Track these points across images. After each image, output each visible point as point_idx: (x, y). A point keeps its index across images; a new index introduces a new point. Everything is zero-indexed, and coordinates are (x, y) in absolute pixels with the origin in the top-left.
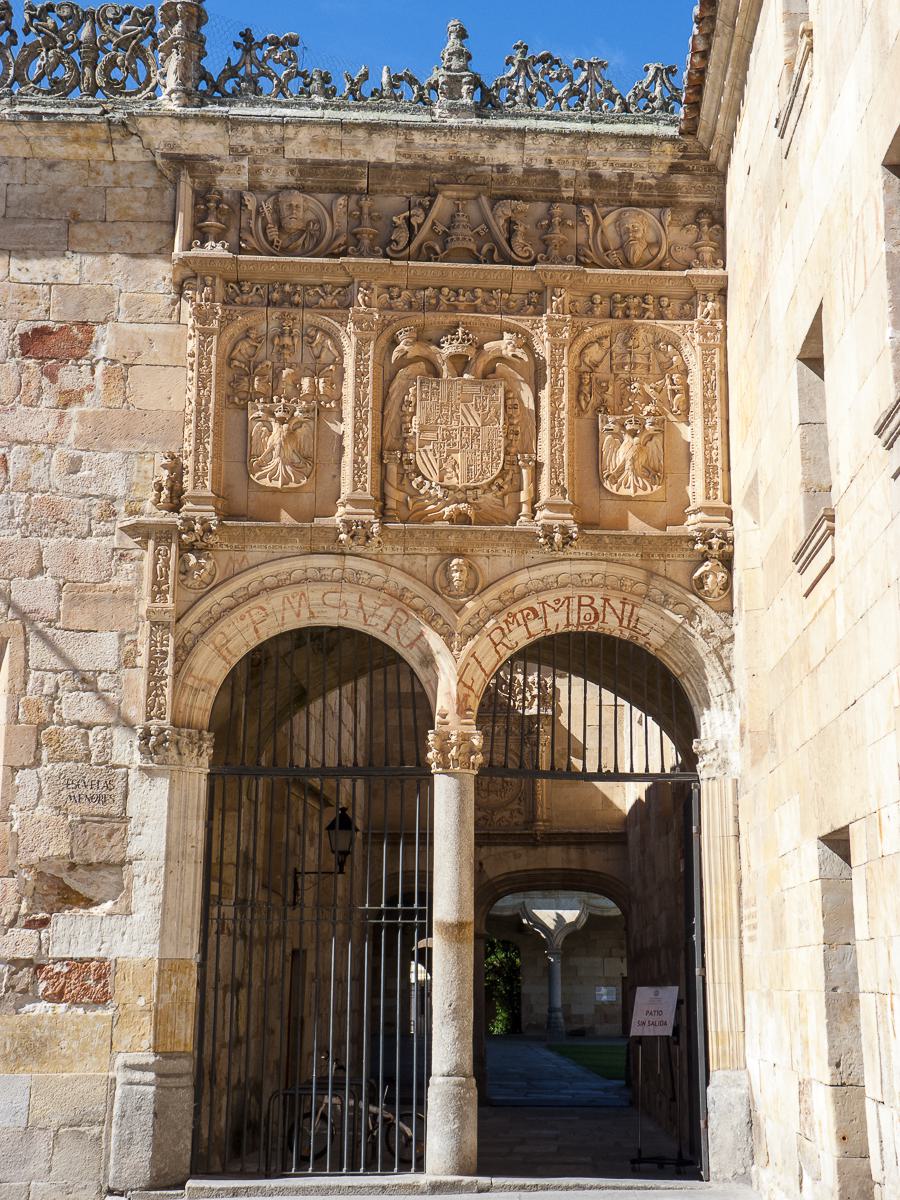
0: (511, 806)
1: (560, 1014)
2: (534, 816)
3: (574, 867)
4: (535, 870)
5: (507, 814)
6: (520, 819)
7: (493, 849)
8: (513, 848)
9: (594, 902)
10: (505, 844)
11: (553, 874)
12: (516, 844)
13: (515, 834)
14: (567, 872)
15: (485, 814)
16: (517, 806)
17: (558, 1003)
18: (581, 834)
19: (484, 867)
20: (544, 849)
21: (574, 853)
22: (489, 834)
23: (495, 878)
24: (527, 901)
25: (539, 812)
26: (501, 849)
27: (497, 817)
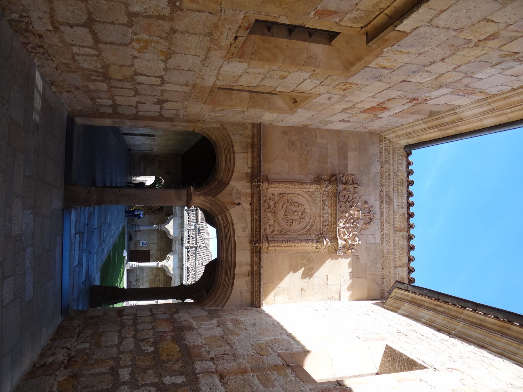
1: (137, 229)
2: (271, 241)
5: (271, 222)
6: (268, 231)
7: (249, 213)
8: (249, 226)
9: (177, 242)
10: (252, 220)
12: (252, 229)
13: (260, 228)
14: (233, 263)
15: (272, 207)
16: (277, 229)
17: (141, 228)
18: (260, 274)
19: (237, 206)
20: (249, 248)
21: (246, 269)
22: (260, 210)
23: (230, 214)
24: (178, 217)
25: (274, 245)
26: (249, 219)
27: (269, 215)
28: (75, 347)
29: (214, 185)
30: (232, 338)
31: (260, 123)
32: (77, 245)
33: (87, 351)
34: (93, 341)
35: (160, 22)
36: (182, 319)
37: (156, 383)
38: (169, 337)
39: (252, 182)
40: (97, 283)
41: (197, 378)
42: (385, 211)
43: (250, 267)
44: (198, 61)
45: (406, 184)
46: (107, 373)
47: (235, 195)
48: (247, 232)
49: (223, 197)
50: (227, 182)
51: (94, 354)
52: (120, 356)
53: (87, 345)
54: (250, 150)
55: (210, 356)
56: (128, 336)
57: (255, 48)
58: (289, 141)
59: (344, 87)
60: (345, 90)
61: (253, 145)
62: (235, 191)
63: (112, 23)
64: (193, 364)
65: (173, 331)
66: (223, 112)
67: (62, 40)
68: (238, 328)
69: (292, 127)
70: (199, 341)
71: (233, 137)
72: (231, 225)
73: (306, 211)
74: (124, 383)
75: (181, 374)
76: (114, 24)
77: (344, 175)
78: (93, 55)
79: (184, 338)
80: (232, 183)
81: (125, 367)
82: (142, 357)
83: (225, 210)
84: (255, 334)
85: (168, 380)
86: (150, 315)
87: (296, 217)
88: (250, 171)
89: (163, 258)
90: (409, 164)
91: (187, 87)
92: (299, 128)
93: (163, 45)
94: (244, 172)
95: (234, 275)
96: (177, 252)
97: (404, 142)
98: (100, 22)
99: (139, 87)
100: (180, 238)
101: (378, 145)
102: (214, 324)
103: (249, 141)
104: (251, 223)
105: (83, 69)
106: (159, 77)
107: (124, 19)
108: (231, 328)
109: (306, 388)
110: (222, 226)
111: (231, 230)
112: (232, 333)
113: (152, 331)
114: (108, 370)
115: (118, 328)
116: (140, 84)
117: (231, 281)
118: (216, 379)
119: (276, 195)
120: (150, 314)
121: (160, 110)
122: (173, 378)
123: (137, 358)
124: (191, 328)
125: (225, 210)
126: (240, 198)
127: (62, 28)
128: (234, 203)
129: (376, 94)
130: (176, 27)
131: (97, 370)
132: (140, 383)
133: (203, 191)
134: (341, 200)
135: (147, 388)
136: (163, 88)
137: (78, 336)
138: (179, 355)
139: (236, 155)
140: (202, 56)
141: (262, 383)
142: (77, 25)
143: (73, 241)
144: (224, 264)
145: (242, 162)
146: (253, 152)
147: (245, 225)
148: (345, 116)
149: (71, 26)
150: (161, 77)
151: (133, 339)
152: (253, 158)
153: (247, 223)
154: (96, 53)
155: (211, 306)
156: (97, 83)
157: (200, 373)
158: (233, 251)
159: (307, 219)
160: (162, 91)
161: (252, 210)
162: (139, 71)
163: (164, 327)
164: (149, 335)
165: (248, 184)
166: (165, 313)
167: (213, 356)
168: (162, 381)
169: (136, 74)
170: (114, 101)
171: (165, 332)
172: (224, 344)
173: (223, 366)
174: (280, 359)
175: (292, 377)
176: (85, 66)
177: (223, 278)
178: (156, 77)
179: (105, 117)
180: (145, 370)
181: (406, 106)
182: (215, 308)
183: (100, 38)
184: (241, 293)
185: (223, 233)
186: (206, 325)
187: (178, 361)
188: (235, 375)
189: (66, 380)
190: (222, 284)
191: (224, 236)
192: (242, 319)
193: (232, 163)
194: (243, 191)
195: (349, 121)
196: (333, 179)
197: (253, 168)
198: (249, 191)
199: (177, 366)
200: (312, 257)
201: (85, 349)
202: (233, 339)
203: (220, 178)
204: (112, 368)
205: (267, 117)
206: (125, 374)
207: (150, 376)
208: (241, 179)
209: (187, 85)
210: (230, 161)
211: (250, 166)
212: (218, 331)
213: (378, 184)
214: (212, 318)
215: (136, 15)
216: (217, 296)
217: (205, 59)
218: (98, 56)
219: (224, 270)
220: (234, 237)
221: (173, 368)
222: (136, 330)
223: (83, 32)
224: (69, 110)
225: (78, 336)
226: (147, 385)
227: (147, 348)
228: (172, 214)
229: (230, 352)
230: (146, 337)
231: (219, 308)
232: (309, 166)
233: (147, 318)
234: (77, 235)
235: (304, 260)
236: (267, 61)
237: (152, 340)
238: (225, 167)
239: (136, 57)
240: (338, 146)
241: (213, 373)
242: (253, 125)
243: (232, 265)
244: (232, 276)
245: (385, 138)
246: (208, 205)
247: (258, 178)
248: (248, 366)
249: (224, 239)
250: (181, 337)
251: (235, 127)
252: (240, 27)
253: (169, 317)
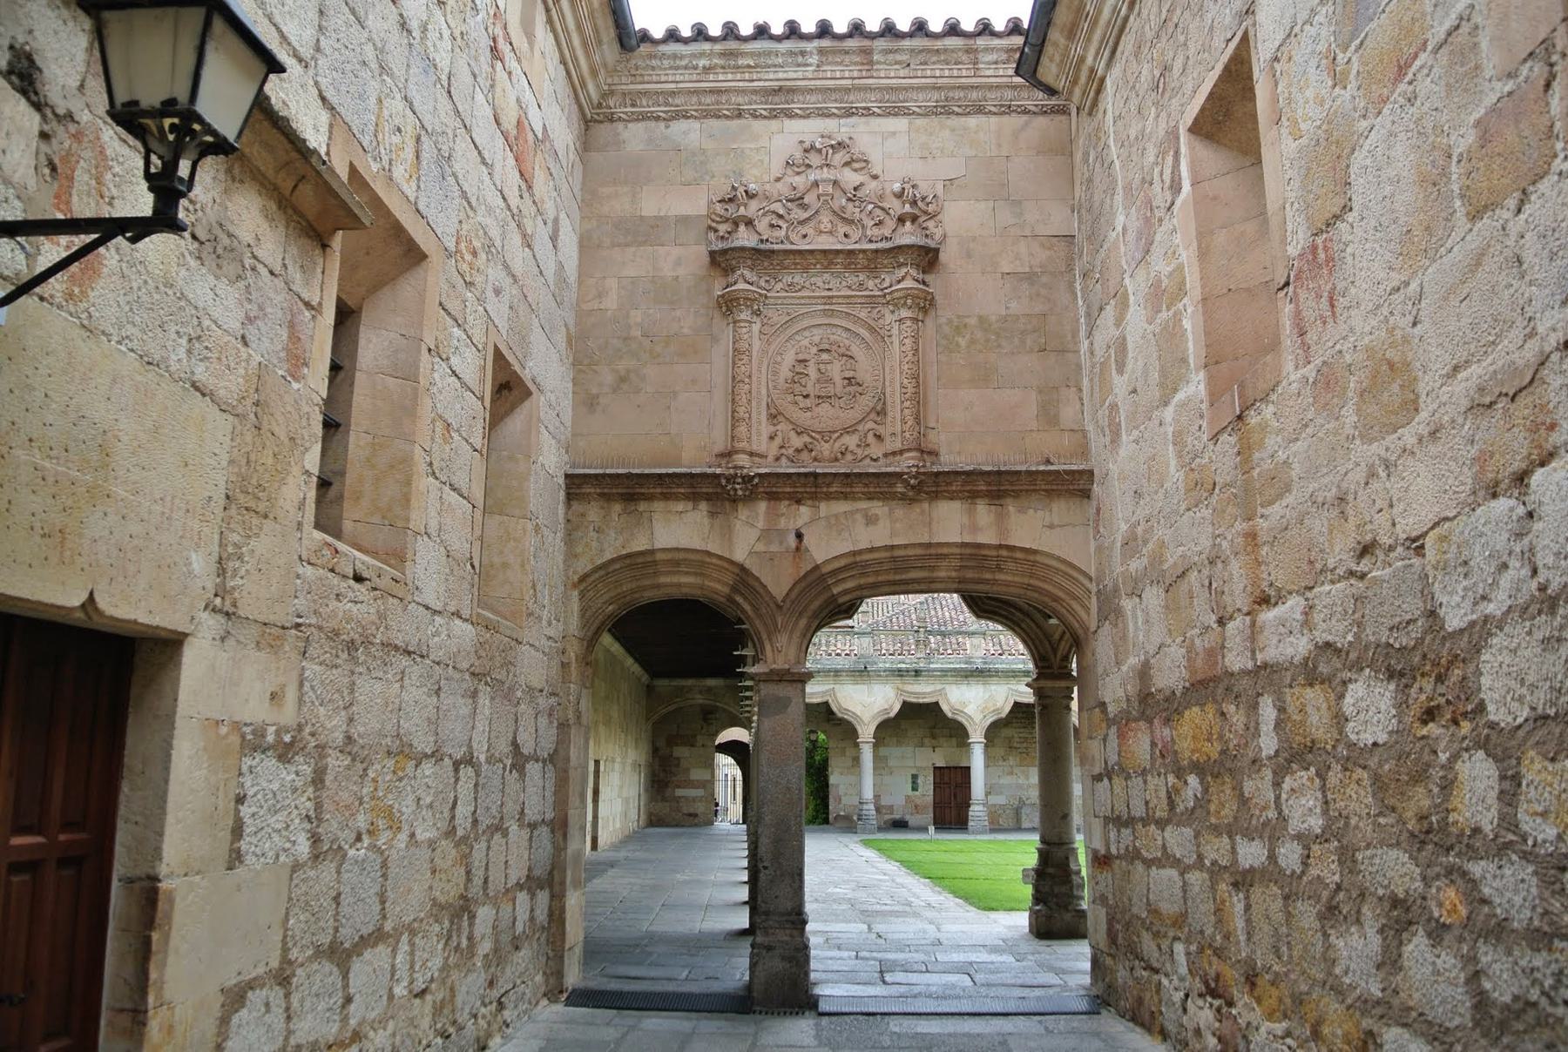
0: (860, 428)
3: (982, 539)
4: (906, 546)
7: (823, 506)
8: (863, 505)
9: (909, 688)
10: (845, 497)
11: (945, 556)
12: (870, 497)
14: (968, 551)
15: (808, 439)
16: (870, 425)
18: (999, 473)
20: (926, 505)
21: (984, 512)
22: (815, 475)
26: (841, 507)
28: (1182, 979)
29: (747, 607)
30: (1171, 561)
31: (567, 476)
32: (913, 978)
33: (1193, 948)
34: (1171, 934)
35: (329, 779)
36: (1121, 693)
37: (1275, 773)
38: (1166, 732)
39: (734, 501)
40: (1022, 920)
41: (1265, 666)
42: (813, 101)
43: (978, 501)
44: (415, 671)
45: (732, 45)
46: (1247, 898)
47: (774, 548)
48: (878, 511)
49: (778, 581)
50: (737, 571)
51: (1202, 932)
52: (1207, 863)
53: (1179, 948)
54: (642, 506)
55: (1215, 626)
56: (1160, 842)
57: (376, 519)
58: (614, 391)
59: (468, 257)
60: (475, 254)
61: (630, 498)
62: (760, 547)
63: (337, 899)
64: (1232, 674)
65: (1150, 721)
66: (539, 587)
67: (382, 1022)
68: (1145, 542)
69: (575, 382)
70: (1176, 652)
71: (608, 556)
72: (858, 559)
73: (816, 339)
74: (1272, 857)
75: (1254, 706)
76: (339, 894)
77: (710, 228)
78: (412, 944)
79: (1168, 693)
80: (740, 555)
81: (1234, 851)
82: (1213, 808)
83: (817, 574)
84: (1161, 495)
85: (1268, 743)
86: (1110, 779)
87: (836, 370)
88: (703, 506)
89: (955, 731)
90: (672, 35)
91: (481, 694)
92: (576, 363)
93: (381, 768)
94: (706, 521)
95: (1000, 546)
96: (939, 687)
97: (610, 51)
98: (336, 930)
99: (485, 821)
100: (898, 681)
101: (620, 126)
102: (1134, 608)
103: (617, 507)
104: (854, 499)
105: (445, 968)
106: (456, 770)
107: (327, 870)
108: (1145, 560)
109: (1292, 378)
110: (862, 581)
111: (876, 555)
112: (1157, 559)
113: (1149, 777)
114: (1241, 895)
115: (1140, 867)
116: (475, 822)
117: (1019, 555)
118: (1268, 616)
119: (772, 429)
120: (1106, 780)
121: (537, 761)
122: (1264, 728)
123: (1213, 820)
124: (1144, 673)
125: (817, 574)
126: (782, 533)
127: (353, 1022)
128: (798, 549)
129: (484, 162)
130: (339, 737)
131: (1240, 924)
132: (1272, 814)
133: (764, 636)
134: (783, 233)
135: (1284, 796)
136: (482, 758)
137: (1157, 971)
138: (1211, 709)
139: (658, 545)
140: (405, 661)
141: (1280, 496)
142: (346, 986)
143: (902, 989)
144: (970, 575)
145: (677, 529)
146: (650, 498)
147: (858, 516)
148: (542, 234)
149: (348, 1000)
150: (457, 765)
151: (1169, 828)
152: (666, 497)
153: (852, 513)
154: (405, 938)
155: (1087, 610)
156: (477, 933)
157: (1254, 658)
158: (933, 551)
159: (840, 336)
160: (490, 760)
161: (815, 497)
162: (443, 825)
163: (1141, 745)
164: (1158, 786)
165: (743, 513)
166: (1105, 740)
167: (1214, 618)
168: (1270, 758)
169: (451, 832)
170: (520, 886)
171: (1153, 744)
172: (1183, 586)
173: (1238, 598)
174: (1224, 437)
175: (1268, 410)
176: (437, 962)
177: (1009, 578)
178: (457, 780)
179: (563, 910)
180: (1244, 801)
181: (512, 64)
182: (1094, 599)
183: (371, 928)
184: (1051, 527)
185: (880, 578)
186: (1136, 629)
187: (1223, 714)
188: (1259, 564)
189: (1259, 1001)
190: (1026, 580)
191: (891, 577)
192: (1124, 527)
193: (681, 556)
194: (761, 524)
195: (556, 220)
196: (722, 261)
197: (694, 497)
198: (762, 506)
199: (1237, 717)
200: (950, 321)
201: (1188, 954)
202: (1171, 559)
203: (726, 590)
204: (1235, 885)
205: (551, 460)
206: (1251, 853)
207: (1258, 789)
208: (728, 534)
209: (474, 694)
210: (677, 563)
211: (690, 505)
212: (1153, 597)
213: (736, 122)
214: (1119, 612)
215: (315, 839)
216: (1061, 594)
217: (409, 653)
218: (413, 933)
219: (988, 576)
220: (892, 547)
221: (1240, 727)
222: (1146, 821)
223: (360, 970)
224: (545, 1002)
225: (1157, 971)
226: (1278, 798)
227: (1190, 793)
228: (826, 704)
229: (1206, 572)
230: (1163, 794)
231: (1094, 589)
232: (686, 331)
233: (1117, 790)
234: (888, 978)
235: (958, 345)
236: (408, 483)
237: (1171, 779)
238: (696, 574)
239: (413, 835)
240: (627, 245)
241: (1253, 623)
242: (570, 498)
243: (974, 554)
244: (1004, 553)
245: (600, 105)
246: (803, 622)
247: (724, 482)
248: (1240, 526)
249: (898, 577)
250: (1167, 700)
251: (579, 550)
252: (332, 570)
253: (1114, 729)
